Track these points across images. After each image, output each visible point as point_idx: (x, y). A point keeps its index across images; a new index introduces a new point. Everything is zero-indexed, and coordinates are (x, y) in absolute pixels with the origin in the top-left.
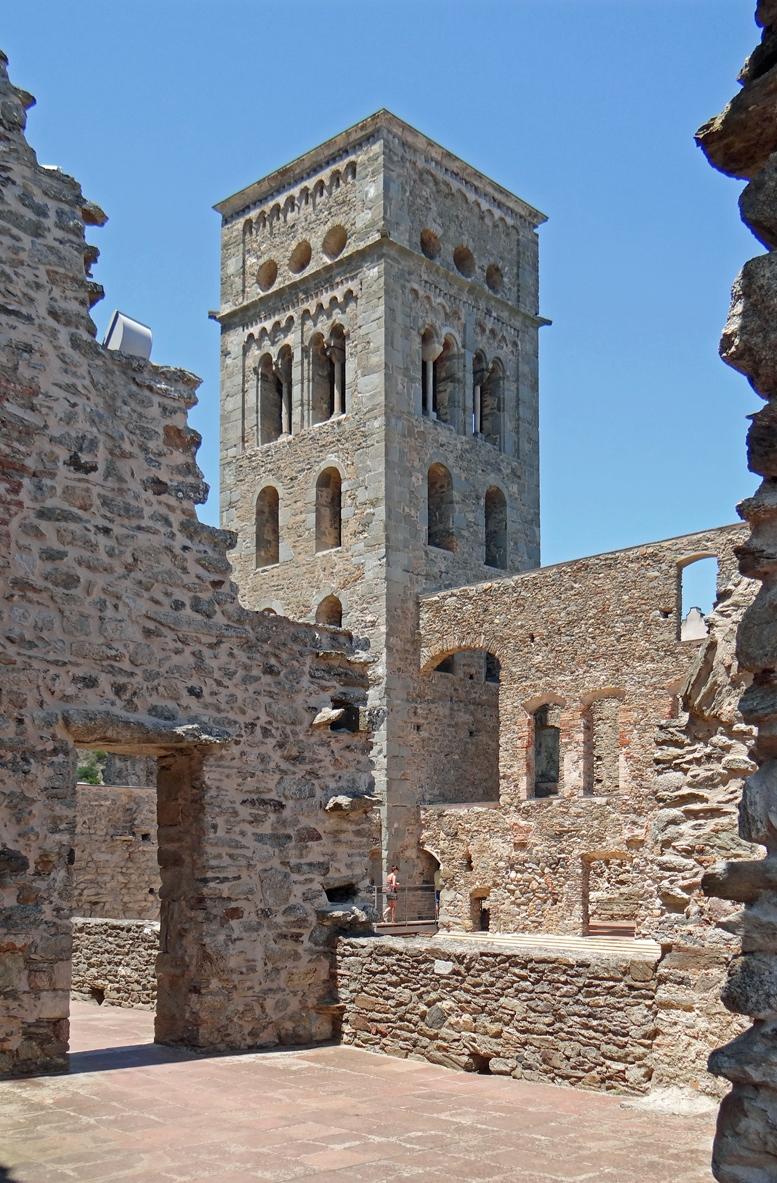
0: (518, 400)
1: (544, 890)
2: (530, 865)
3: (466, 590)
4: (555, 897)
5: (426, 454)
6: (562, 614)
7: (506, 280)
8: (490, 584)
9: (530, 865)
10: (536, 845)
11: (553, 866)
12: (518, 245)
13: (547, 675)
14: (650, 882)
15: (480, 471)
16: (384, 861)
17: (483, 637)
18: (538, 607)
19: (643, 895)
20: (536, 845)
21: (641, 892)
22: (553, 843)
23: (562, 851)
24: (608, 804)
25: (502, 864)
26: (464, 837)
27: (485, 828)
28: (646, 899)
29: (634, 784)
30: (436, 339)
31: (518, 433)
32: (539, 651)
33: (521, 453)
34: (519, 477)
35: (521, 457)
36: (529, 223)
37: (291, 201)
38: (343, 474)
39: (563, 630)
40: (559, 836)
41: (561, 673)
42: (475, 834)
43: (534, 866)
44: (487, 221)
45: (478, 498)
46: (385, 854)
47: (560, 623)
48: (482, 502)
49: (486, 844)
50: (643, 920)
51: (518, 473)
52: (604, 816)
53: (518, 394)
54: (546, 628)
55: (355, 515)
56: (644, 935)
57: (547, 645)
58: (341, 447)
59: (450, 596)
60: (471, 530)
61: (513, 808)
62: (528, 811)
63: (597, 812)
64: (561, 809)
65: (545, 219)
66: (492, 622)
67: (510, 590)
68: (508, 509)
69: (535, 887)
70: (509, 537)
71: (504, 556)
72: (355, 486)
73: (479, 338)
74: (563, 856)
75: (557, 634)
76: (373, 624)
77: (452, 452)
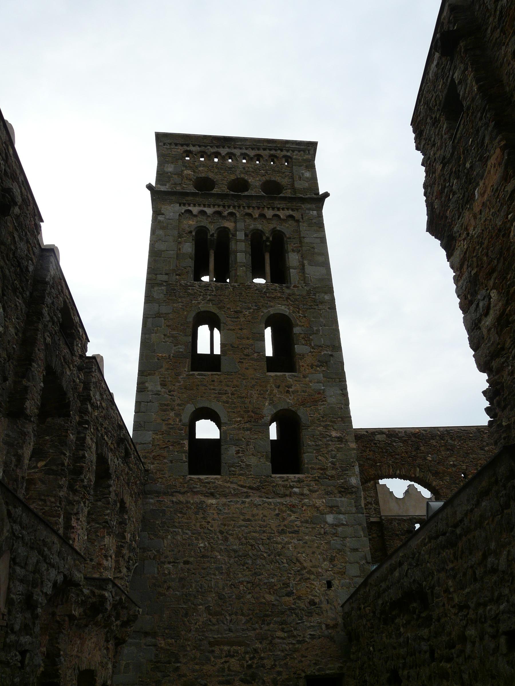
18: (466, 453)
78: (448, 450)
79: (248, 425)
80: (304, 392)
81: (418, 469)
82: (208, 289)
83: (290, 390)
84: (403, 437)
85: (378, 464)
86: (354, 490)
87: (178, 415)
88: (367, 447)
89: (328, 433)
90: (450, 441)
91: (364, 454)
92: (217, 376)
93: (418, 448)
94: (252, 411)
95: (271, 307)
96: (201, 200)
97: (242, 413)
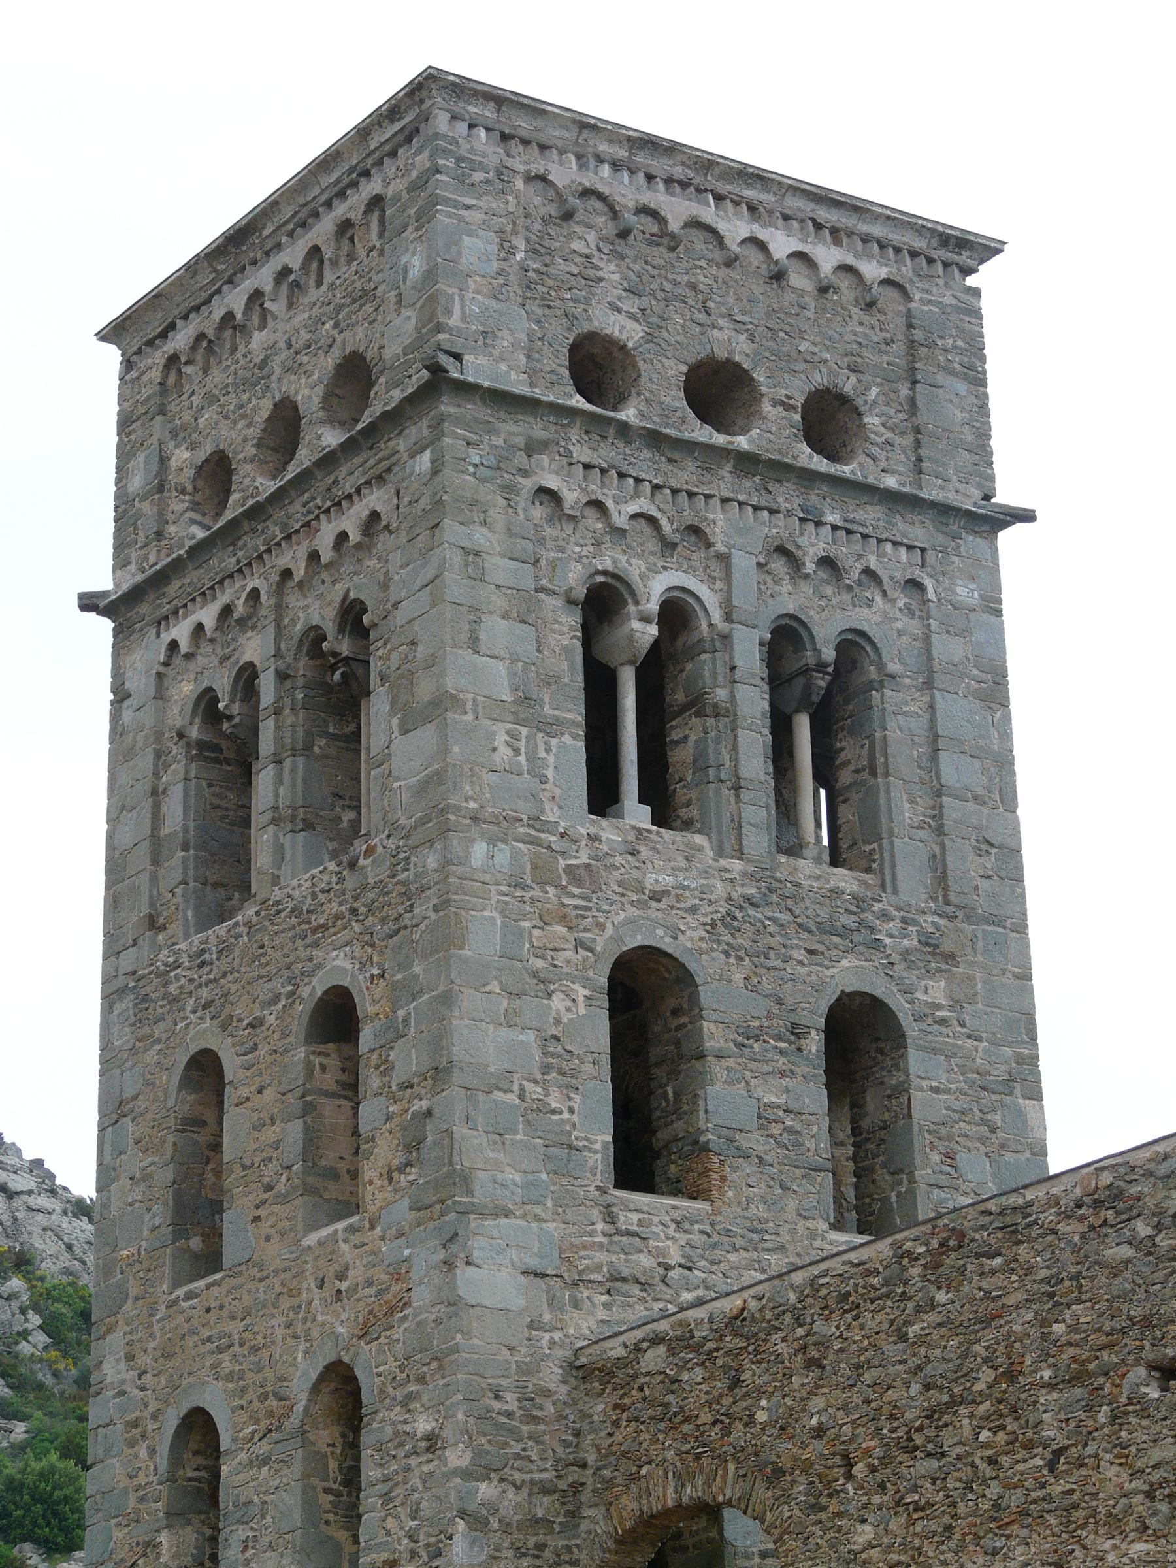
0: (934, 738)
5: (601, 927)
7: (872, 420)
12: (910, 326)
15: (799, 955)
17: (731, 1467)
18: (858, 1367)
30: (632, 608)
31: (940, 831)
33: (953, 887)
34: (950, 957)
35: (953, 897)
36: (946, 265)
37: (256, 296)
38: (366, 1006)
39: (918, 1439)
44: (798, 279)
45: (797, 1032)
48: (815, 1043)
51: (947, 946)
53: (933, 721)
55: (389, 1118)
57: (882, 1486)
58: (357, 927)
60: (776, 1129)
65: (988, 249)
66: (750, 1422)
67: (787, 1318)
68: (911, 1051)
70: (921, 1141)
71: (909, 1197)
72: (390, 1035)
73: (786, 587)
75: (905, 1450)
76: (432, 1443)
77: (693, 910)
78: (811, 1363)
79: (264, 1448)
80: (369, 1283)
81: (731, 1467)
82: (203, 964)
83: (344, 1286)
85: (644, 1471)
87: (152, 1451)
89: (407, 1428)
90: (819, 1326)
92: (215, 1290)
93: (736, 1383)
94: (275, 1394)
95: (319, 967)
96: (196, 574)
97: (256, 1404)
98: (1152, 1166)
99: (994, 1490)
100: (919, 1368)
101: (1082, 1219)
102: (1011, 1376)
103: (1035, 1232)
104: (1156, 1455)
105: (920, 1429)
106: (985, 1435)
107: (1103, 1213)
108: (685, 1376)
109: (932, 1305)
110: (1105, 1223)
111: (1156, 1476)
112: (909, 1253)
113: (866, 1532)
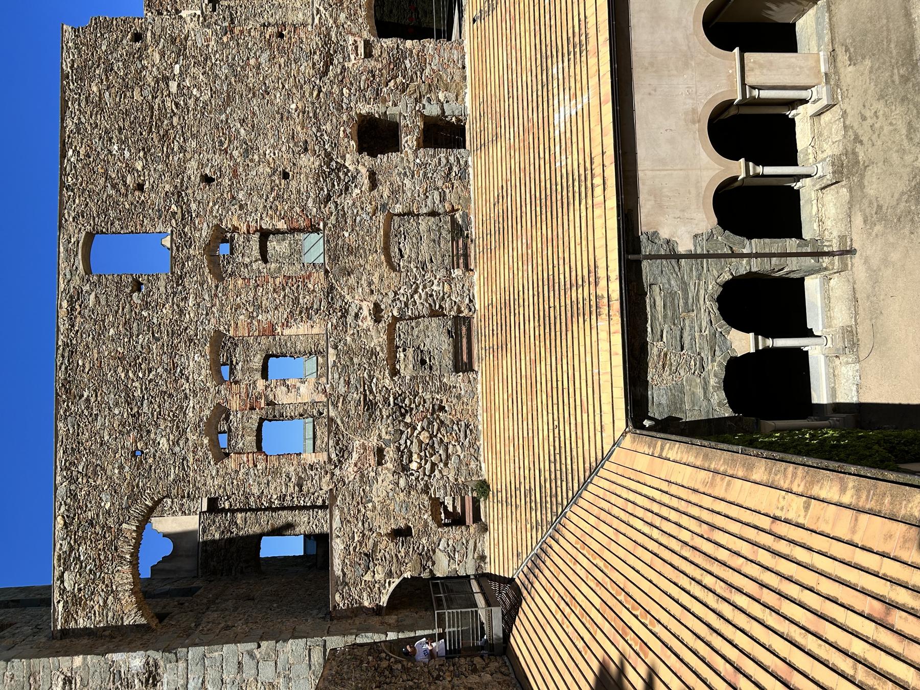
1: (430, 423)
2: (402, 442)
3: (59, 556)
4: (436, 407)
6: (116, 412)
8: (59, 519)
9: (402, 442)
10: (380, 436)
11: (403, 411)
13: (185, 431)
14: (416, 297)
16: (401, 636)
18: (101, 445)
19: (430, 305)
20: (380, 436)
21: (428, 305)
22: (378, 413)
23: (386, 400)
24: (336, 347)
25: (402, 482)
26: (370, 543)
27: (359, 511)
28: (434, 300)
29: (315, 318)
32: (154, 442)
40: (370, 406)
41: (185, 413)
42: (366, 525)
43: (404, 436)
46: (392, 636)
47: (125, 415)
49: (379, 508)
50: (455, 302)
52: (349, 352)
54: (129, 432)
56: (471, 301)
59: (62, 582)
61: (337, 472)
62: (341, 449)
63: (345, 360)
64: (340, 405)
66: (108, 512)
67: (73, 487)
69: (427, 434)
74: (391, 399)
78: (95, 473)
81: (124, 526)
84: (69, 543)
86: (151, 662)
88: (86, 604)
91: (96, 608)
93: (91, 523)
98: (66, 281)
99: (160, 370)
100: (110, 409)
101: (76, 317)
102: (122, 358)
103: (74, 342)
104: (162, 289)
105: (131, 409)
106: (141, 375)
107: (77, 307)
108: (82, 558)
109: (88, 400)
110: (80, 306)
111: (170, 291)
112: (66, 411)
113: (163, 441)
